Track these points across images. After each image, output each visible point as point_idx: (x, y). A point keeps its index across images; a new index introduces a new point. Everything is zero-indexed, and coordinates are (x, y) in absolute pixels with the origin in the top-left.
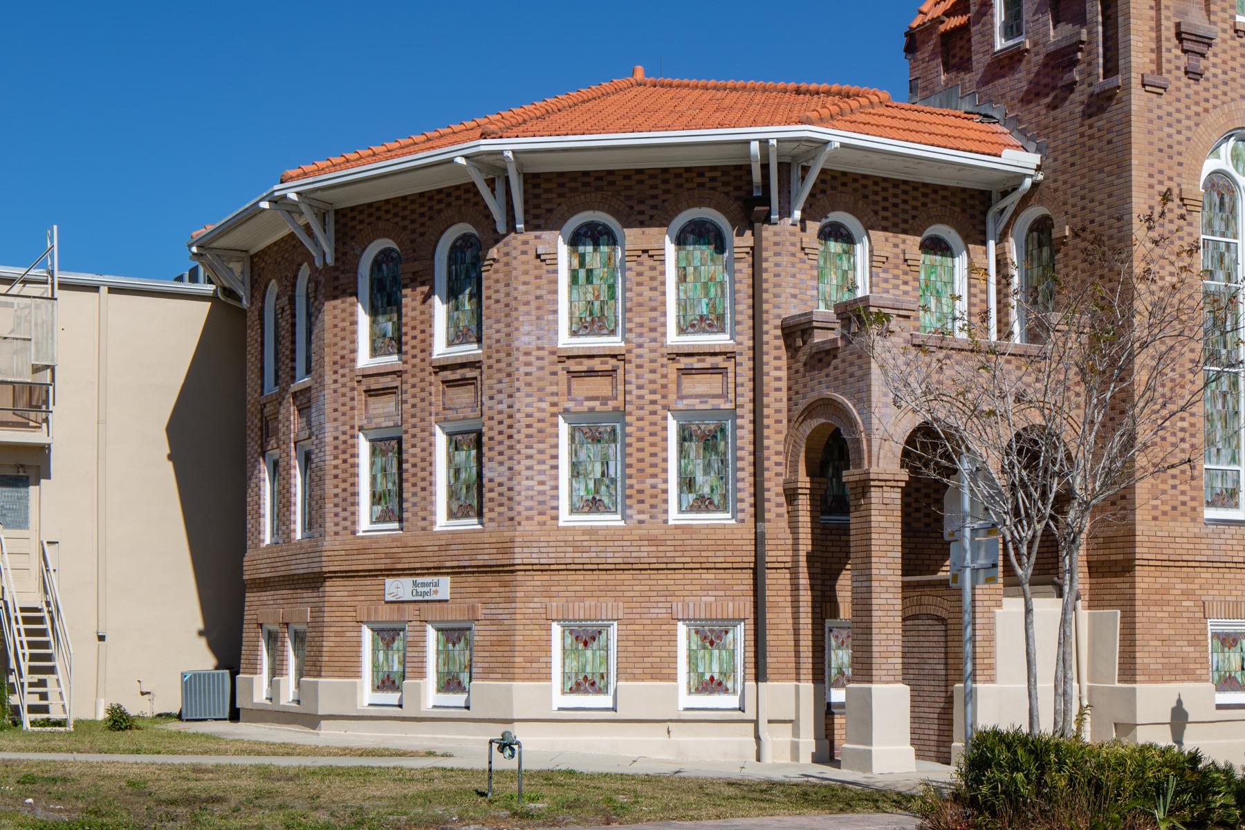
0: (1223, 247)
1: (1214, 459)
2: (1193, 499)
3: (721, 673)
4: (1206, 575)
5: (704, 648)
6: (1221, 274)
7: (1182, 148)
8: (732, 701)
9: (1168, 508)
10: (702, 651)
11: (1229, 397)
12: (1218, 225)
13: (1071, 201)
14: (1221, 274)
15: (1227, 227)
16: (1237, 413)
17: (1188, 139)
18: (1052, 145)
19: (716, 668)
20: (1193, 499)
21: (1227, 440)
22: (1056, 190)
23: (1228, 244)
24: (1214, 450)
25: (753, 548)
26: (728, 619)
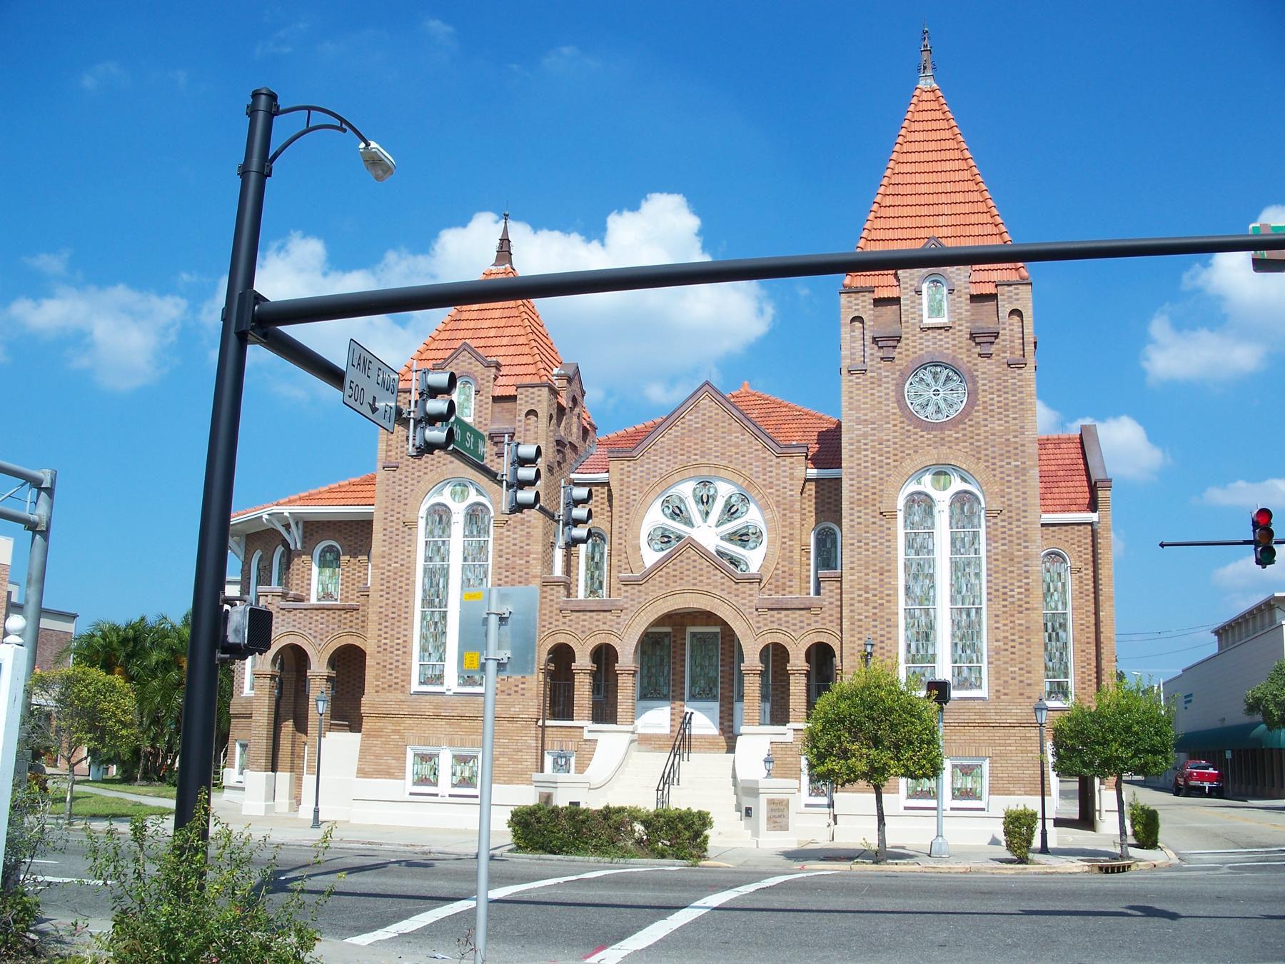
0: (440, 544)
1: (426, 659)
2: (403, 681)
4: (408, 721)
6: (438, 558)
7: (407, 496)
9: (386, 686)
11: (439, 624)
15: (443, 532)
16: (444, 633)
17: (412, 490)
20: (403, 681)
21: (437, 648)
23: (444, 542)
24: (427, 654)
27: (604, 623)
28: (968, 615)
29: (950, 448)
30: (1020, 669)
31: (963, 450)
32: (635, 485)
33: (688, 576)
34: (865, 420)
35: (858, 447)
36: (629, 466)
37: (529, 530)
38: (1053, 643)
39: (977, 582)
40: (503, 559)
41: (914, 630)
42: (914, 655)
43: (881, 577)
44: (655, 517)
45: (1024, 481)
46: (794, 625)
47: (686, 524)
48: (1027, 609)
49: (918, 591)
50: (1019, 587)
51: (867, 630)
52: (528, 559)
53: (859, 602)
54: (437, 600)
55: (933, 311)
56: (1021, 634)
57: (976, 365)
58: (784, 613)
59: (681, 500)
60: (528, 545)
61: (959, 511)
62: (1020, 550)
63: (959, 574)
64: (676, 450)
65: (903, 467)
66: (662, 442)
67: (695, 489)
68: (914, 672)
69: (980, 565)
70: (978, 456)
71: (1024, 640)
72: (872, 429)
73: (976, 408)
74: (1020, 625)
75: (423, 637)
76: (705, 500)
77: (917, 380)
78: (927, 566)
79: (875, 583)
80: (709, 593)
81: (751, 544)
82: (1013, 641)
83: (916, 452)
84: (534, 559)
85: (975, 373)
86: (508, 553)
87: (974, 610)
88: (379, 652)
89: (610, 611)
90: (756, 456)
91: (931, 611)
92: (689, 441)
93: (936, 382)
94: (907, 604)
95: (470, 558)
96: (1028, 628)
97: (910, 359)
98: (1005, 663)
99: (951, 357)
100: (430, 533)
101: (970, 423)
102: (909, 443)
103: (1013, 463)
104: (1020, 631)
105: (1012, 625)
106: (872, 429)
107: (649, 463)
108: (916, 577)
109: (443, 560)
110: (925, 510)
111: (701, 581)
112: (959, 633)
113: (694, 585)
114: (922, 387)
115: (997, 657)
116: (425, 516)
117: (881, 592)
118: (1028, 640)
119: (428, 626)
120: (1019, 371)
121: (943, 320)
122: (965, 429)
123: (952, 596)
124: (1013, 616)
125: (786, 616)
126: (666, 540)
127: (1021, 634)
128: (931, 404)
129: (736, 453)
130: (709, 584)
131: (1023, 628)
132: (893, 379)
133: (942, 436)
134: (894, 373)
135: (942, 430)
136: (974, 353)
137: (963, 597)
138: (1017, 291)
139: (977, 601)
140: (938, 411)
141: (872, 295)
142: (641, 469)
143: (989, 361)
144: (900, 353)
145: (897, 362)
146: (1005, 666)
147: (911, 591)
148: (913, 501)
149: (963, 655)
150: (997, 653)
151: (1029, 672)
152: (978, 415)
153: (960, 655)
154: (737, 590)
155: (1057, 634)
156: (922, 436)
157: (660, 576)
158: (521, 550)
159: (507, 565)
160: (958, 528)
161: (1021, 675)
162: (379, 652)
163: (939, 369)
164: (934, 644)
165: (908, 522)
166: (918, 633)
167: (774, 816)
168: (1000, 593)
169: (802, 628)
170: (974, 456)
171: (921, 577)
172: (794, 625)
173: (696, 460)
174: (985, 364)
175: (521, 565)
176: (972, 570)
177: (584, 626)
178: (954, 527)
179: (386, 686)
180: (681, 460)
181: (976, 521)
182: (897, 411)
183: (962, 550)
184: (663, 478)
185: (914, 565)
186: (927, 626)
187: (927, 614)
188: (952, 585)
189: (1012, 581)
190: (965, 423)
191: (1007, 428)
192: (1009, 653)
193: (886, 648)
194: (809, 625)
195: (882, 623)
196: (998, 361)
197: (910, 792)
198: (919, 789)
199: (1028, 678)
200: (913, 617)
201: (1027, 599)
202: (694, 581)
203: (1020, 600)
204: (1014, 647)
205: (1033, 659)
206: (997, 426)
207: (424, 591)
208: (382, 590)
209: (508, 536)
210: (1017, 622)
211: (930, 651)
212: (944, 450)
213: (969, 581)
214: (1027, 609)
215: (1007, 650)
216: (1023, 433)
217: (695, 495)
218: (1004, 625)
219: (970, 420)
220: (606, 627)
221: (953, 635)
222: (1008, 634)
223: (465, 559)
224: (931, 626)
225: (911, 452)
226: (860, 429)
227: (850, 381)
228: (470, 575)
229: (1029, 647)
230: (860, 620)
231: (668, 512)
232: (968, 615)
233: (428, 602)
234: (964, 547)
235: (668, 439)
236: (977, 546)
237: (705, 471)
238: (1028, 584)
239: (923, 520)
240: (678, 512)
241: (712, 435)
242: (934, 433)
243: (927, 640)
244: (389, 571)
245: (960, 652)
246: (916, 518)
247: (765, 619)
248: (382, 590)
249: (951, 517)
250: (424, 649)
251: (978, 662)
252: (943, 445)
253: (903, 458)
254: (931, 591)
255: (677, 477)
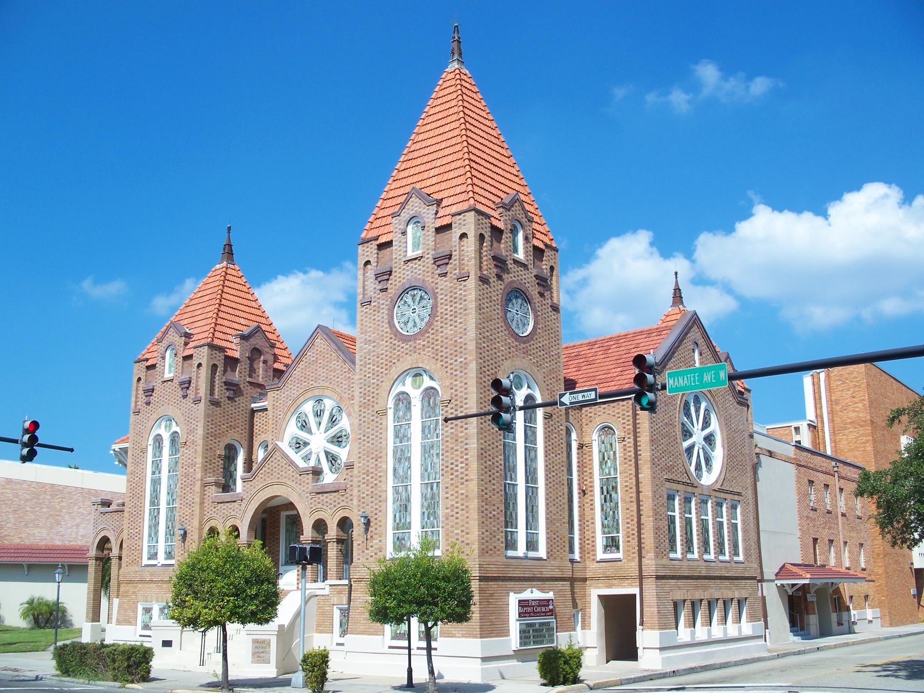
6: (157, 472)
12: (158, 454)
14: (157, 472)
27: (234, 510)
28: (432, 489)
29: (419, 354)
30: (462, 531)
31: (428, 354)
32: (280, 408)
33: (275, 472)
34: (370, 341)
35: (365, 362)
36: (277, 395)
37: (195, 448)
38: (608, 504)
39: (438, 461)
40: (184, 469)
41: (398, 503)
42: (398, 524)
43: (376, 463)
44: (292, 429)
45: (466, 374)
46: (331, 504)
47: (308, 433)
48: (467, 481)
49: (401, 472)
50: (462, 463)
51: (368, 505)
52: (195, 468)
53: (364, 483)
54: (156, 501)
55: (415, 246)
56: (462, 502)
57: (437, 284)
58: (325, 495)
59: (306, 416)
60: (195, 458)
61: (427, 404)
62: (462, 432)
63: (427, 455)
64: (302, 379)
65: (390, 374)
66: (295, 374)
67: (313, 407)
68: (398, 538)
69: (439, 446)
70: (437, 357)
71: (464, 507)
72: (374, 347)
73: (436, 319)
74: (462, 494)
75: (150, 527)
76: (319, 414)
77: (403, 303)
78: (406, 451)
79: (372, 468)
80: (284, 484)
81: (344, 444)
82: (457, 508)
83: (398, 360)
84: (198, 468)
85: (436, 291)
86: (186, 465)
87: (435, 484)
88: (128, 539)
89: (235, 501)
90: (345, 376)
91: (409, 486)
92: (309, 371)
93: (414, 302)
94: (394, 483)
95: (171, 470)
96: (467, 496)
97: (397, 287)
98: (452, 526)
99: (421, 280)
100: (154, 455)
101: (432, 331)
102: (394, 354)
103: (459, 360)
104: (462, 499)
105: (456, 494)
106: (374, 347)
107: (288, 391)
108: (400, 460)
109: (160, 473)
110: (406, 406)
111: (282, 475)
112: (426, 504)
113: (278, 478)
114: (406, 307)
115: (447, 522)
116: (152, 444)
117: (376, 475)
118: (467, 507)
119: (152, 519)
120: (464, 283)
121: (419, 253)
122: (428, 337)
123: (422, 474)
124: (457, 487)
125: (327, 498)
126: (298, 445)
127: (462, 502)
128: (410, 321)
129: (334, 376)
130: (286, 477)
131: (464, 497)
132: (387, 305)
133: (415, 345)
134: (387, 301)
135: (415, 340)
136: (436, 275)
137: (429, 474)
138: (464, 218)
139: (438, 476)
140: (415, 326)
141: (375, 243)
142: (283, 395)
143: (445, 279)
144: (391, 284)
145: (389, 291)
146: (452, 529)
147: (397, 471)
148: (399, 400)
149: (428, 521)
150: (447, 519)
151: (467, 533)
152: (437, 324)
153: (426, 522)
154: (300, 480)
155: (611, 495)
156: (402, 348)
157: (262, 474)
158: (192, 462)
159: (186, 473)
160: (426, 418)
161: (463, 536)
162: (128, 539)
163: (416, 292)
164: (410, 514)
165: (396, 417)
166: (401, 505)
167: (258, 652)
168: (449, 469)
169: (335, 506)
170: (433, 358)
171: (403, 461)
172: (331, 504)
173: (312, 385)
174: (443, 282)
175: (192, 472)
176: (433, 452)
177: (224, 513)
178: (424, 417)
179: (130, 562)
180: (305, 386)
181: (437, 411)
182: (388, 330)
183: (429, 436)
184: (295, 401)
185: (399, 450)
186: (406, 500)
187: (406, 490)
188: (422, 465)
189: (457, 458)
190: (429, 332)
191: (456, 331)
192: (454, 518)
193: (378, 519)
194: (339, 503)
195: (376, 499)
196: (451, 277)
197: (393, 634)
198: (398, 632)
199: (467, 539)
200: (397, 493)
201: (466, 472)
202: (278, 476)
203: (462, 473)
204: (457, 513)
205: (470, 522)
206: (448, 331)
207: (151, 494)
208: (130, 497)
209: (186, 453)
210: (460, 492)
211: (408, 520)
212: (415, 356)
213: (432, 461)
214: (467, 481)
215: (453, 516)
216: (465, 334)
217: (313, 411)
218: (452, 495)
219: (433, 329)
220: (233, 513)
221: (422, 506)
222: (454, 503)
223: (169, 472)
224: (409, 500)
225: (395, 361)
226: (366, 348)
227: (362, 311)
228: (171, 482)
229: (467, 512)
230: (364, 498)
231: (299, 425)
232: (432, 489)
233: (152, 503)
234: (430, 433)
235: (299, 371)
236: (438, 432)
237: (317, 392)
238: (467, 459)
239: (405, 414)
240: (304, 424)
241: (321, 365)
242: (410, 343)
243: (406, 511)
244: (134, 483)
245: (426, 519)
246: (401, 413)
247: (315, 501)
248: (130, 497)
249: (422, 410)
250: (150, 535)
251: (437, 527)
252: (415, 352)
253: (391, 366)
254: (409, 470)
255: (302, 399)
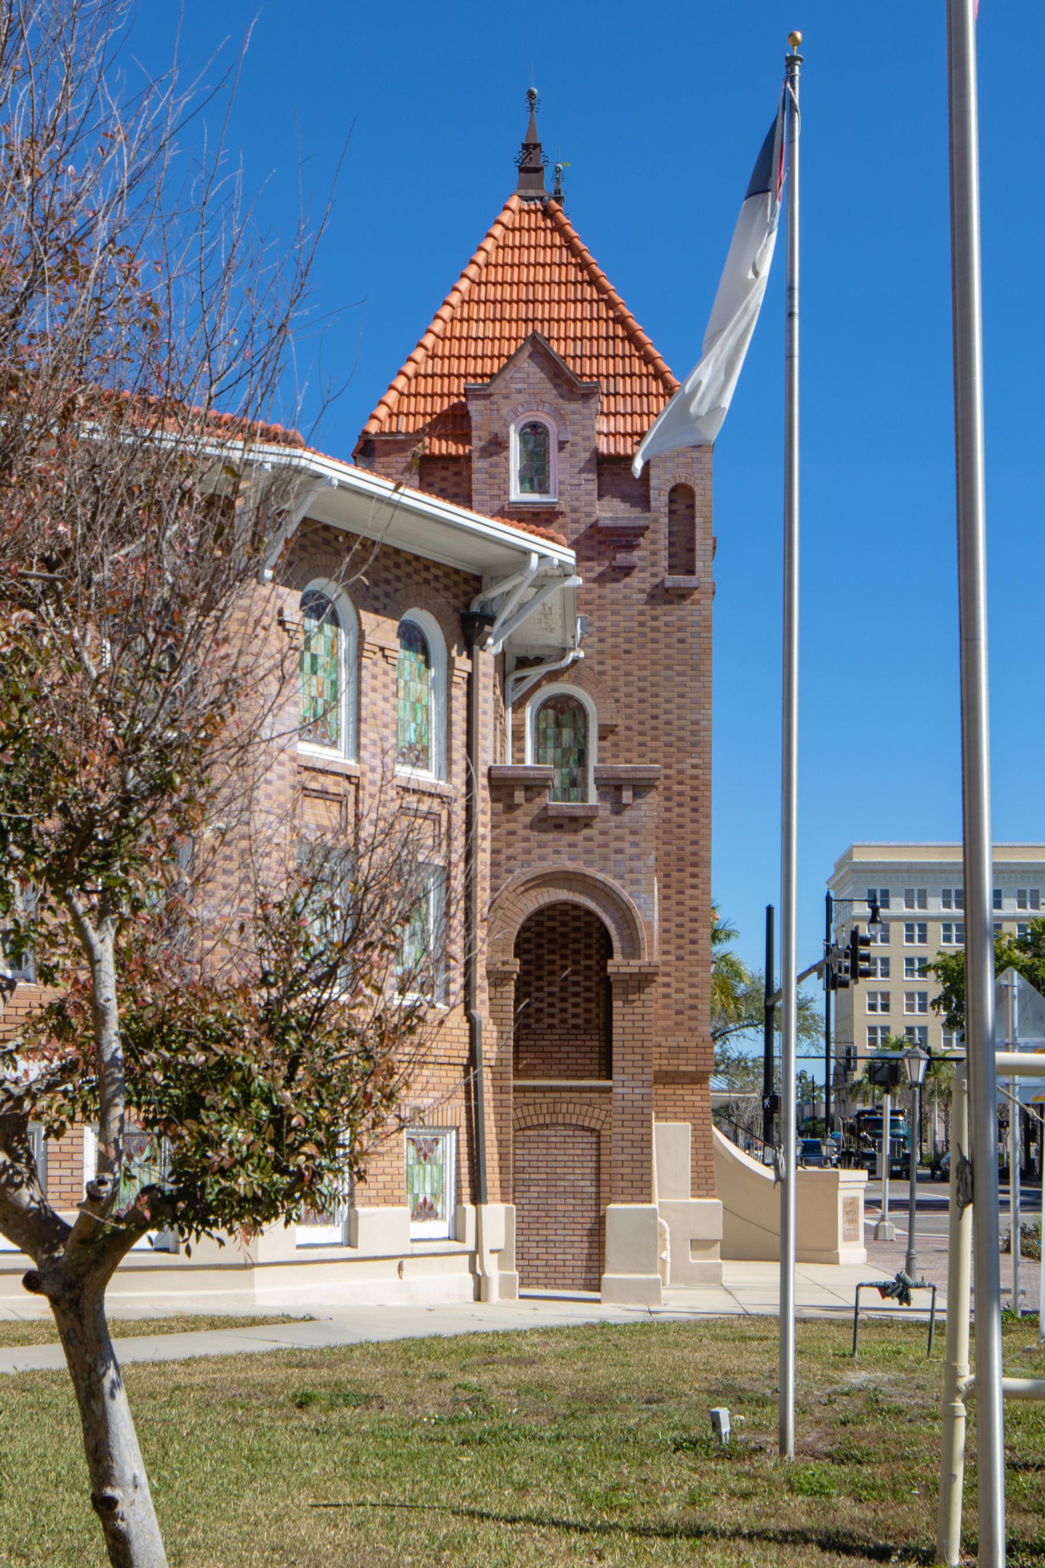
3: (432, 1194)
5: (419, 1163)
8: (440, 1228)
10: (417, 1168)
13: (624, 689)
18: (597, 624)
19: (428, 1189)
22: (602, 673)
25: (467, 1040)
26: (442, 1127)
